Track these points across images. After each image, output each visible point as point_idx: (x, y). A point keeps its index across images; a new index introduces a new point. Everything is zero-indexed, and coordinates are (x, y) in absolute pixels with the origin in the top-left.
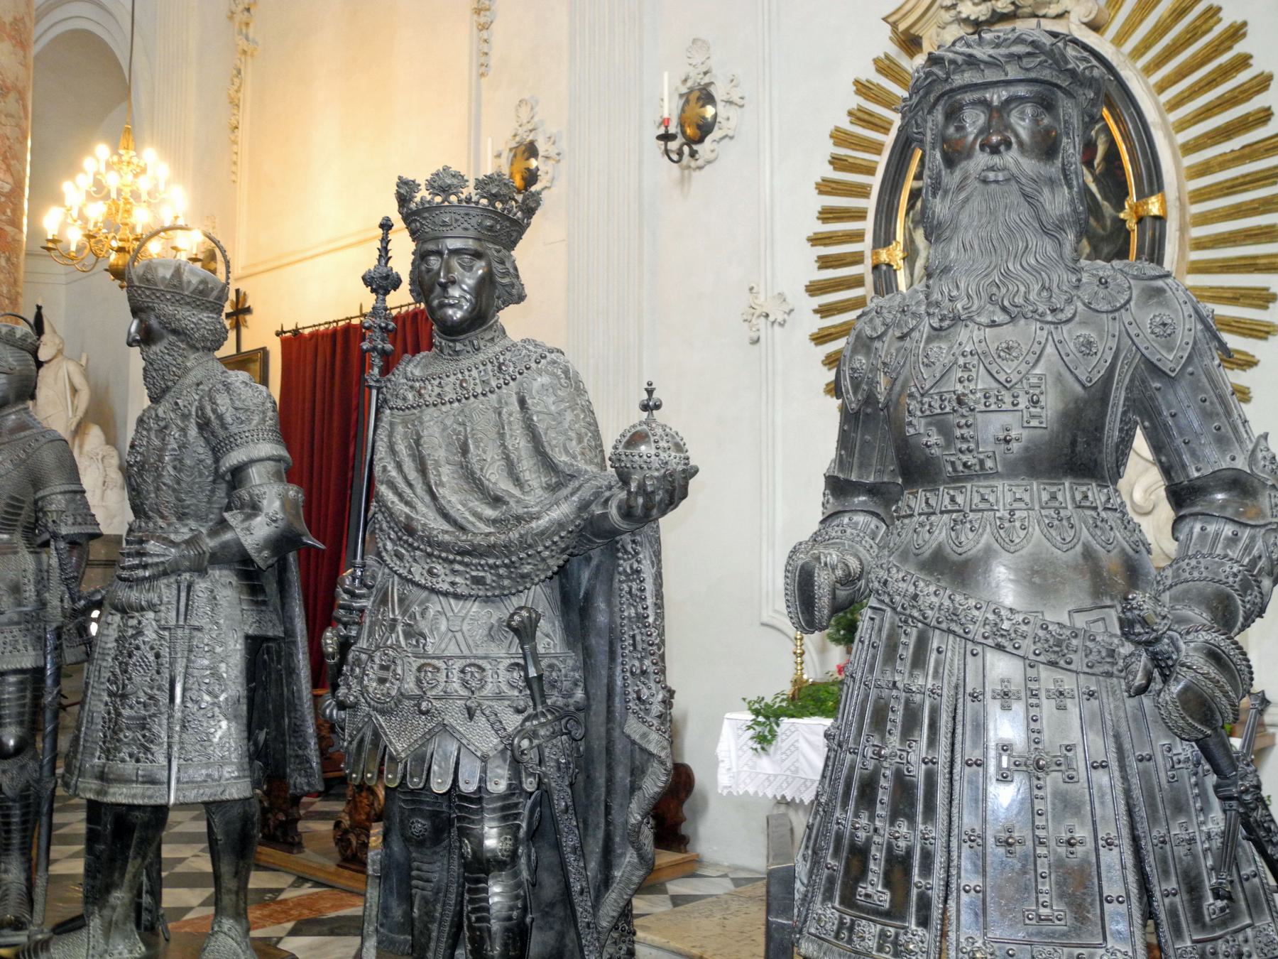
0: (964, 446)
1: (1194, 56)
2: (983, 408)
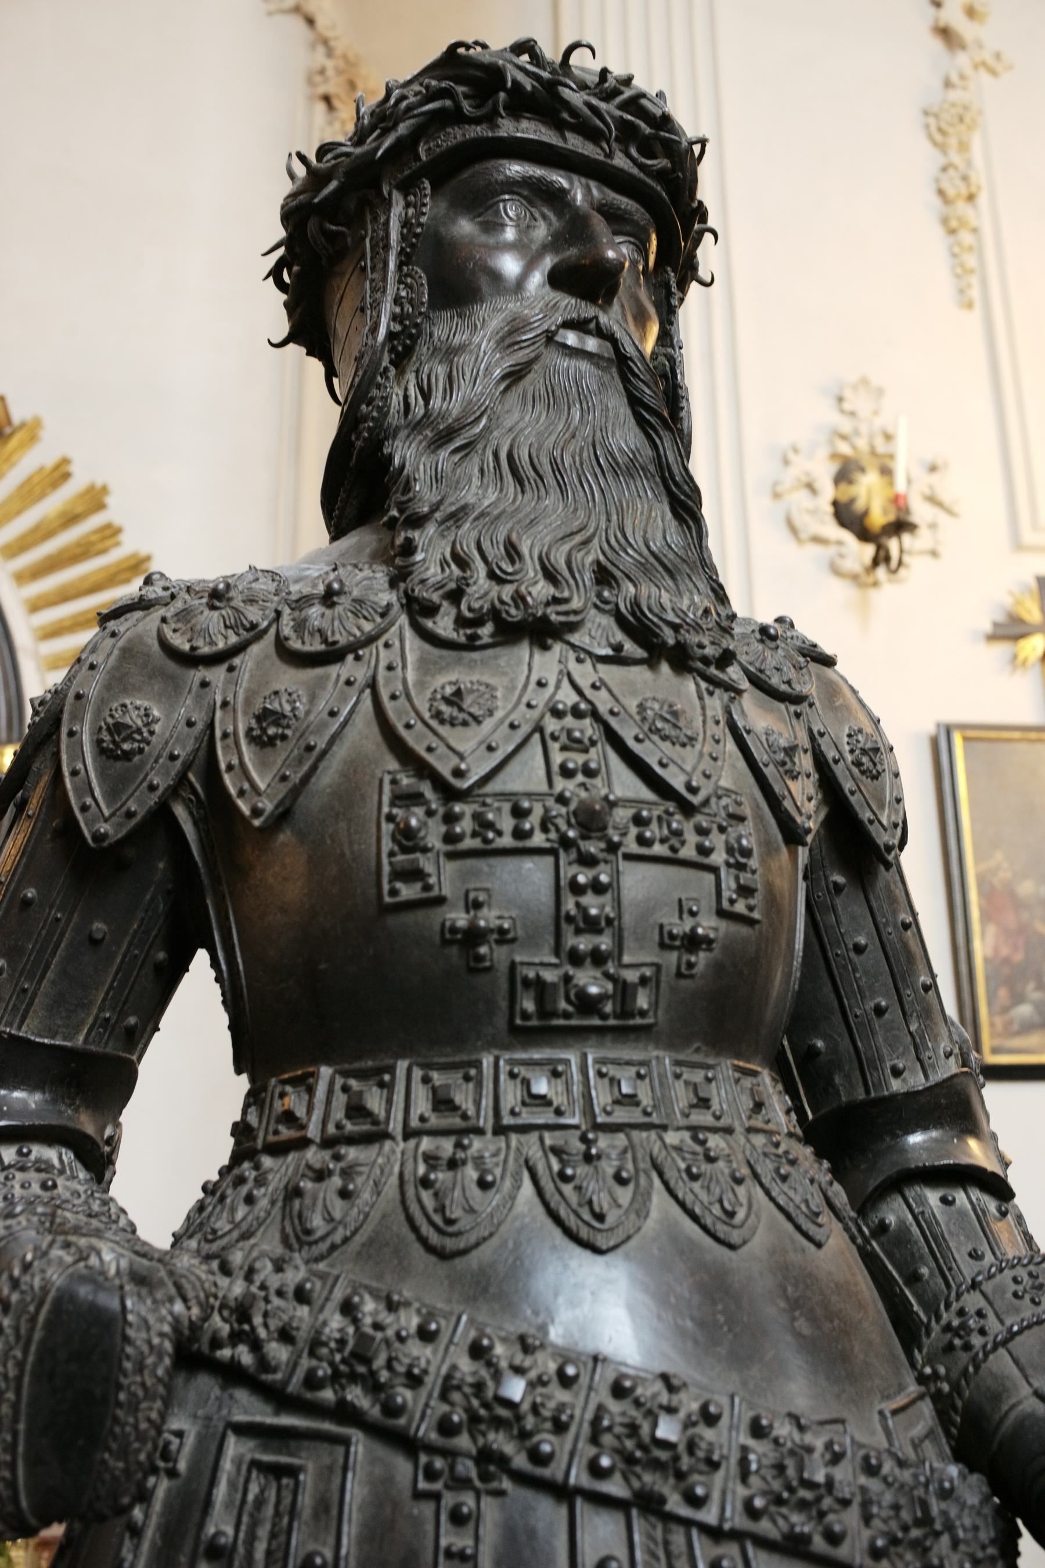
0: (584, 944)
1: (84, 578)
2: (633, 848)
